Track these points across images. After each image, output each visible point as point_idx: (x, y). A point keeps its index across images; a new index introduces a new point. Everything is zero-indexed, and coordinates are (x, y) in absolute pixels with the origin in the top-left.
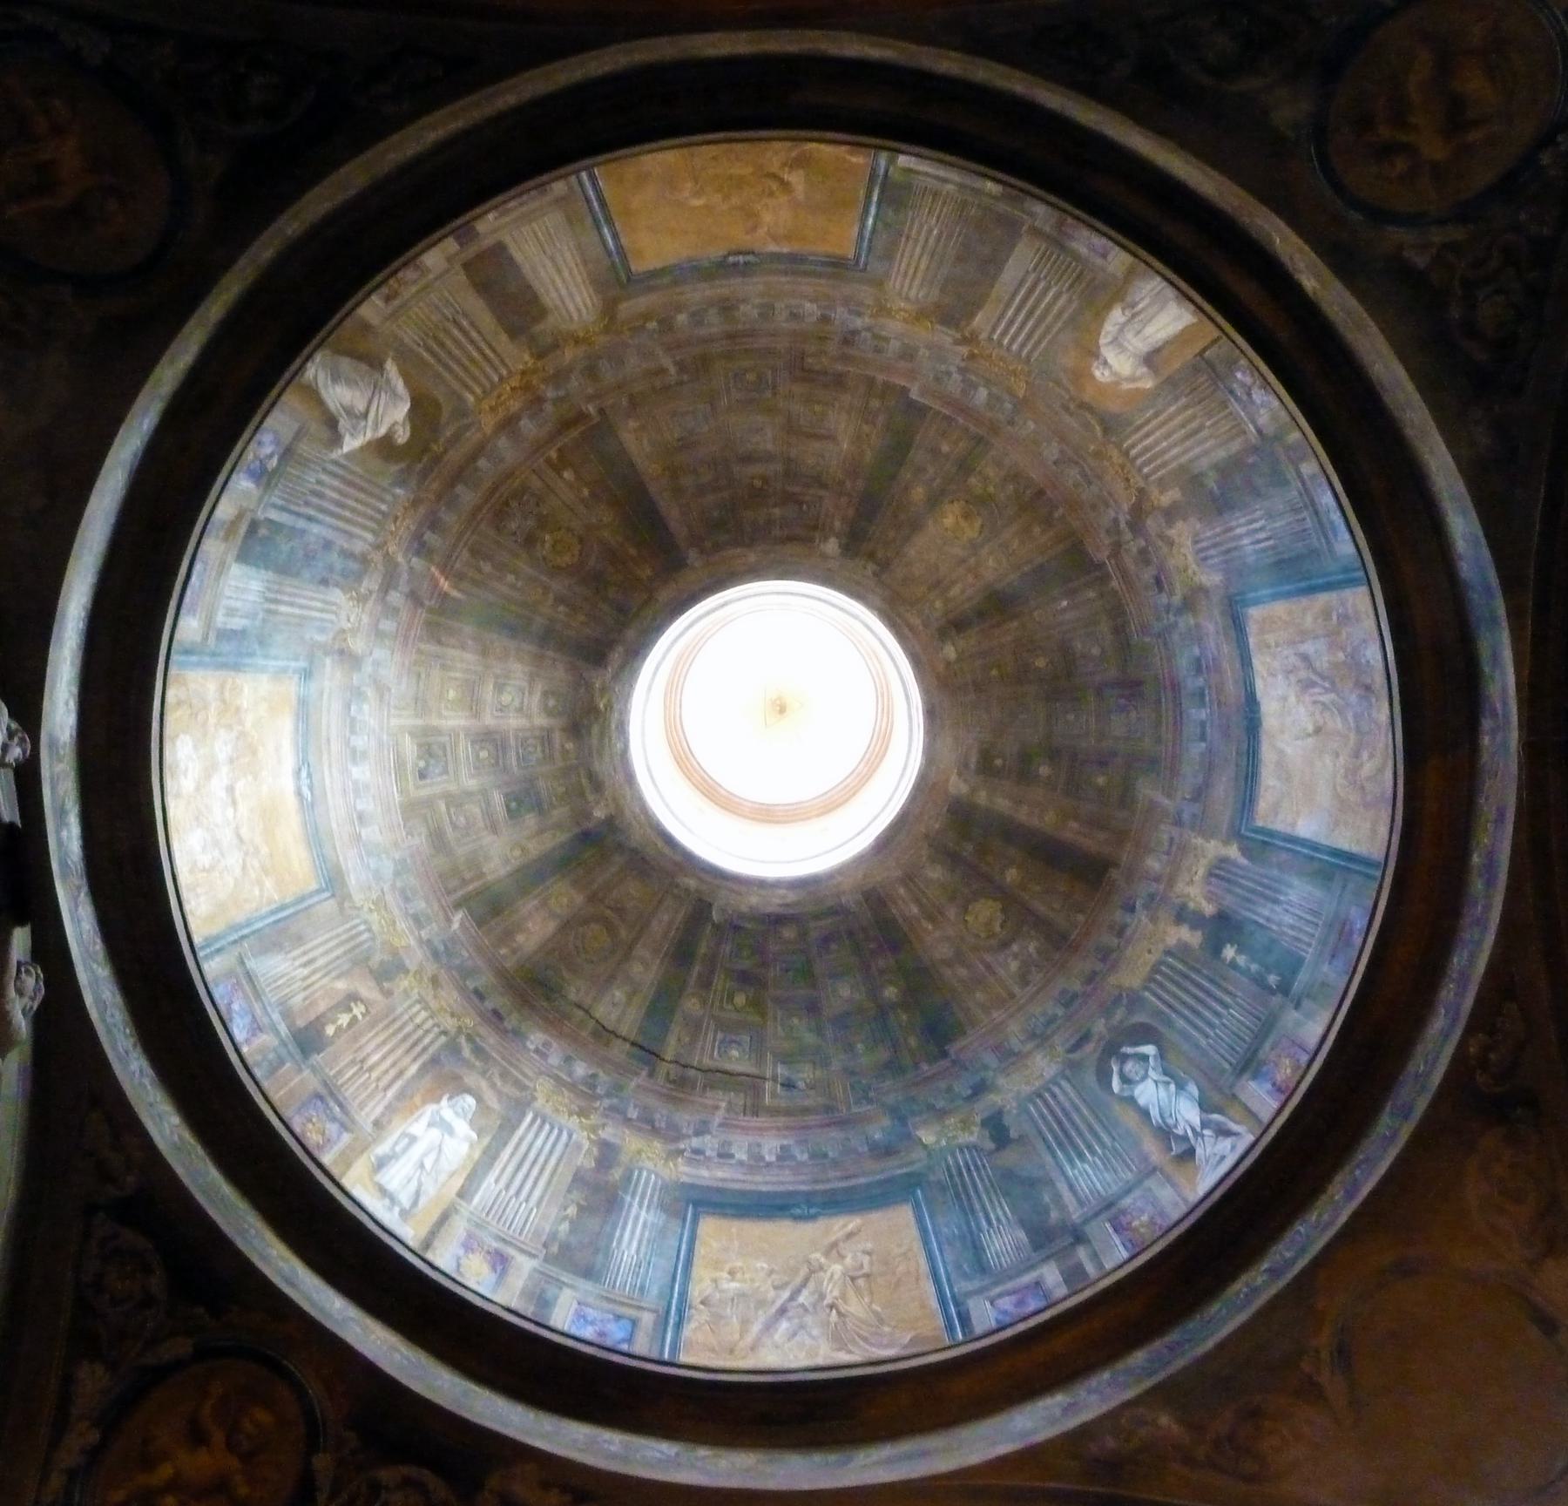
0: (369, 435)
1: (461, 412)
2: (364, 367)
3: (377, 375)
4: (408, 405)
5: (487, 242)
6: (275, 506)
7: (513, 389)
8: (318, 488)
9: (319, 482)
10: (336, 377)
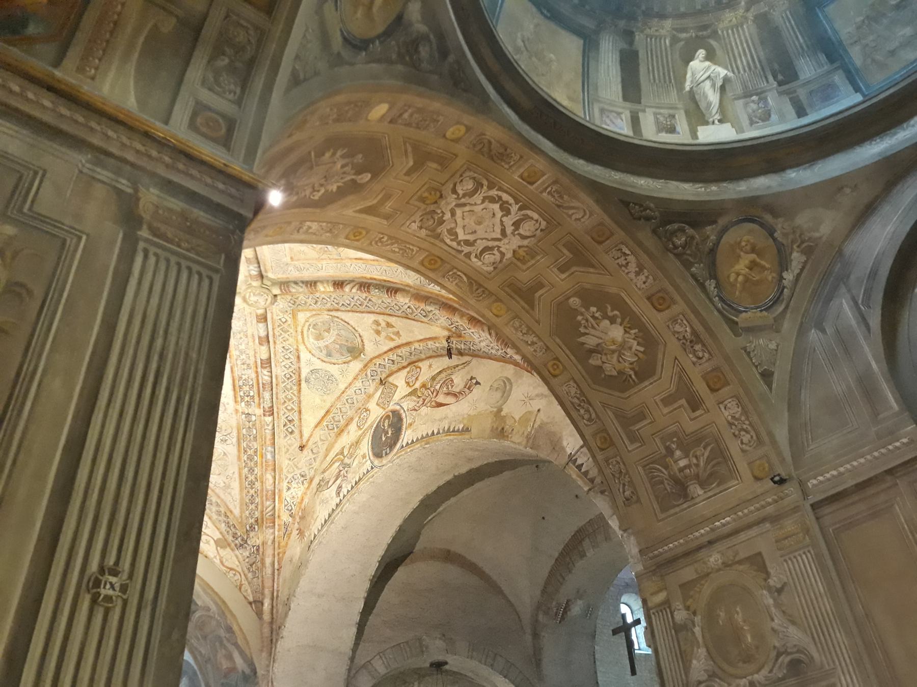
0: (713, 67)
1: (675, 40)
2: (697, 97)
3: (695, 89)
4: (691, 63)
5: (628, 105)
6: (768, 82)
7: (650, 28)
8: (747, 69)
9: (745, 71)
10: (709, 104)
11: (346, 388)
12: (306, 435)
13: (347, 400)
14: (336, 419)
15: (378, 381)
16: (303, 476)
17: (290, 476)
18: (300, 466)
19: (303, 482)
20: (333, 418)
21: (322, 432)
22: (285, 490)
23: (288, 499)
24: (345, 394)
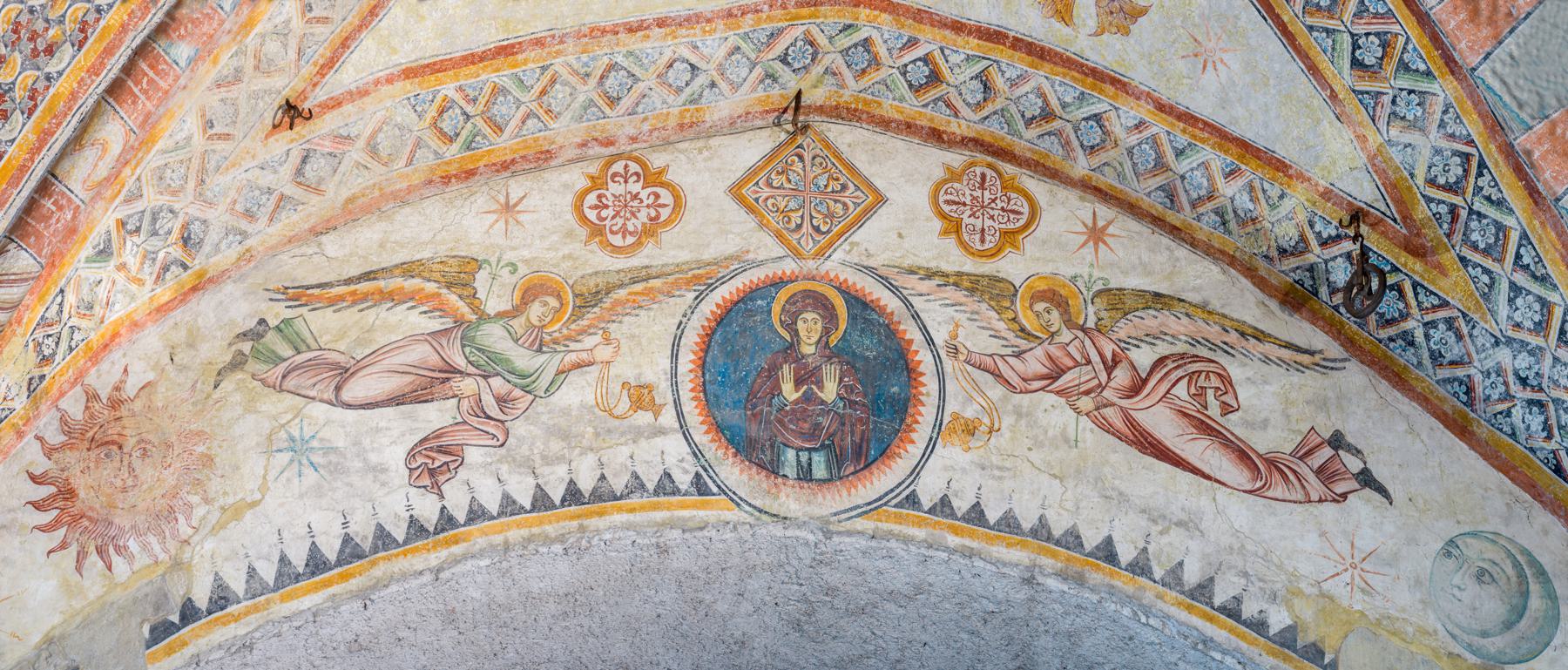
11: (661, 23)
12: (347, 76)
13: (612, 67)
14: (501, 109)
15: (779, 95)
16: (186, 241)
17: (152, 198)
18: (219, 182)
19: (166, 269)
20: (499, 91)
21: (405, 115)
22: (87, 251)
23: (71, 298)
24: (634, 43)
